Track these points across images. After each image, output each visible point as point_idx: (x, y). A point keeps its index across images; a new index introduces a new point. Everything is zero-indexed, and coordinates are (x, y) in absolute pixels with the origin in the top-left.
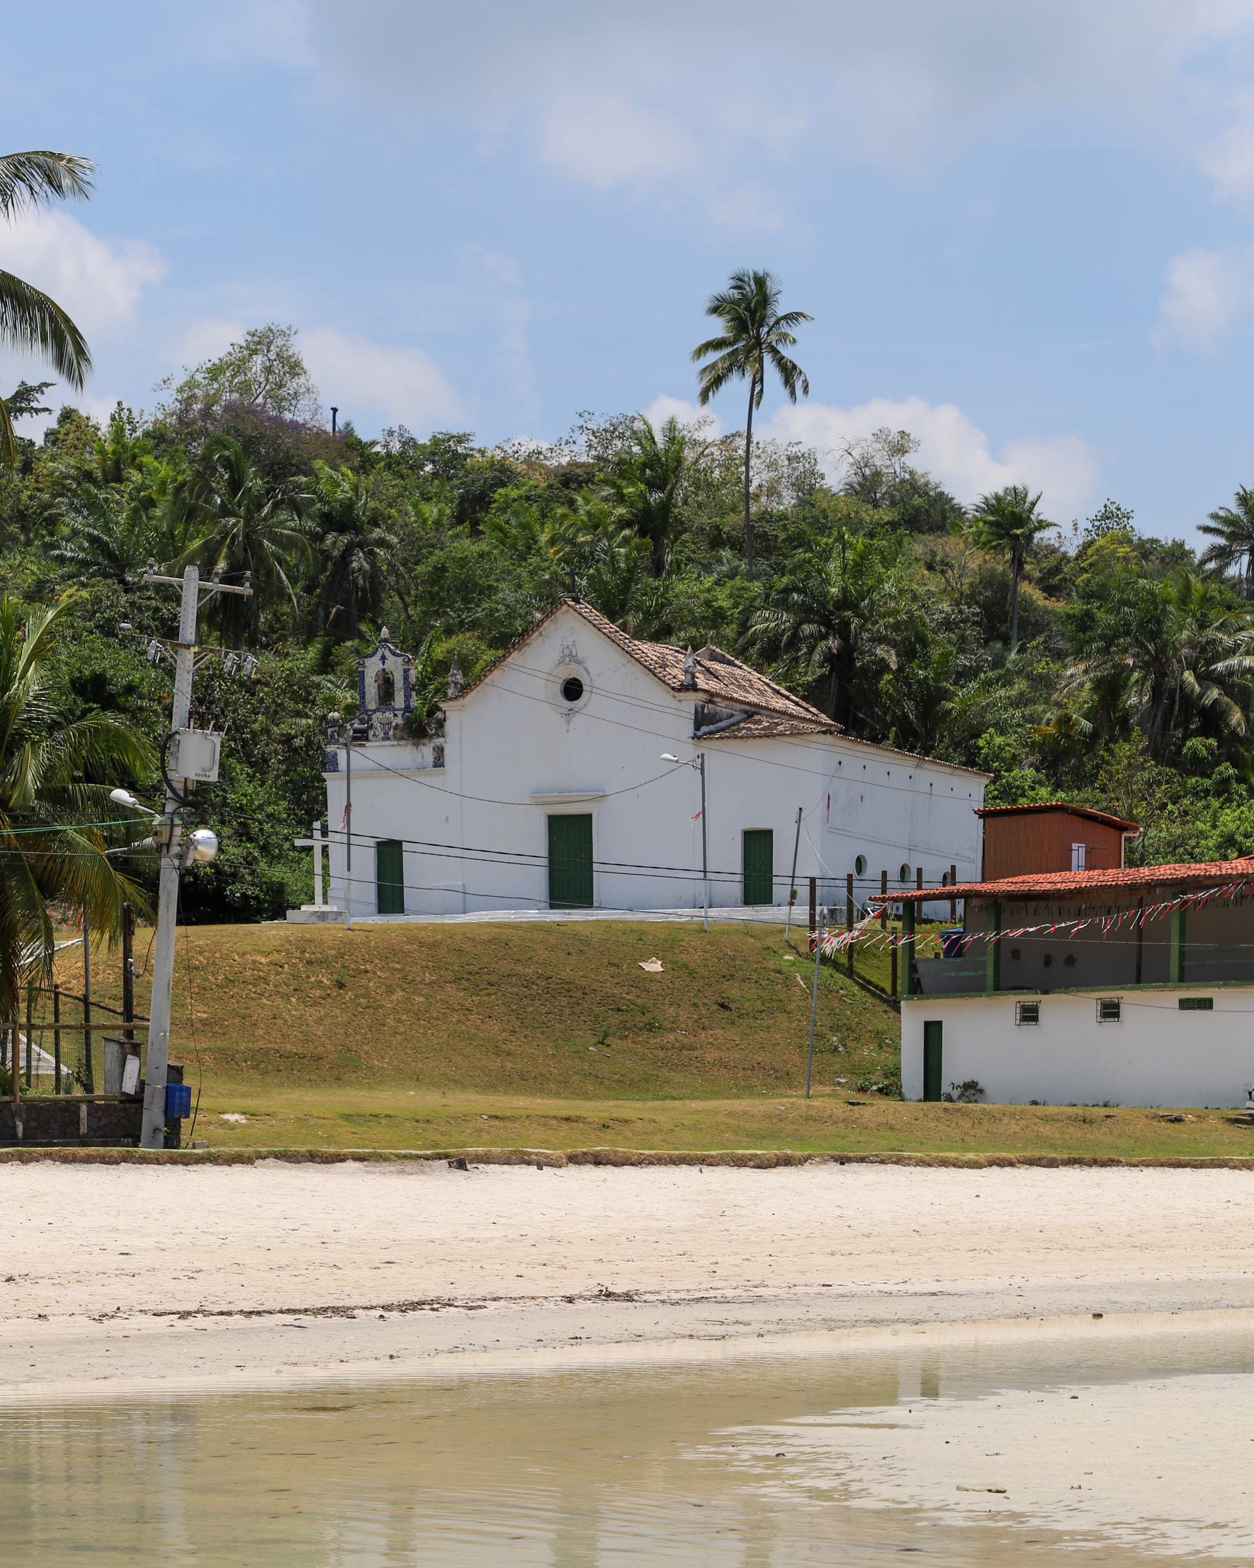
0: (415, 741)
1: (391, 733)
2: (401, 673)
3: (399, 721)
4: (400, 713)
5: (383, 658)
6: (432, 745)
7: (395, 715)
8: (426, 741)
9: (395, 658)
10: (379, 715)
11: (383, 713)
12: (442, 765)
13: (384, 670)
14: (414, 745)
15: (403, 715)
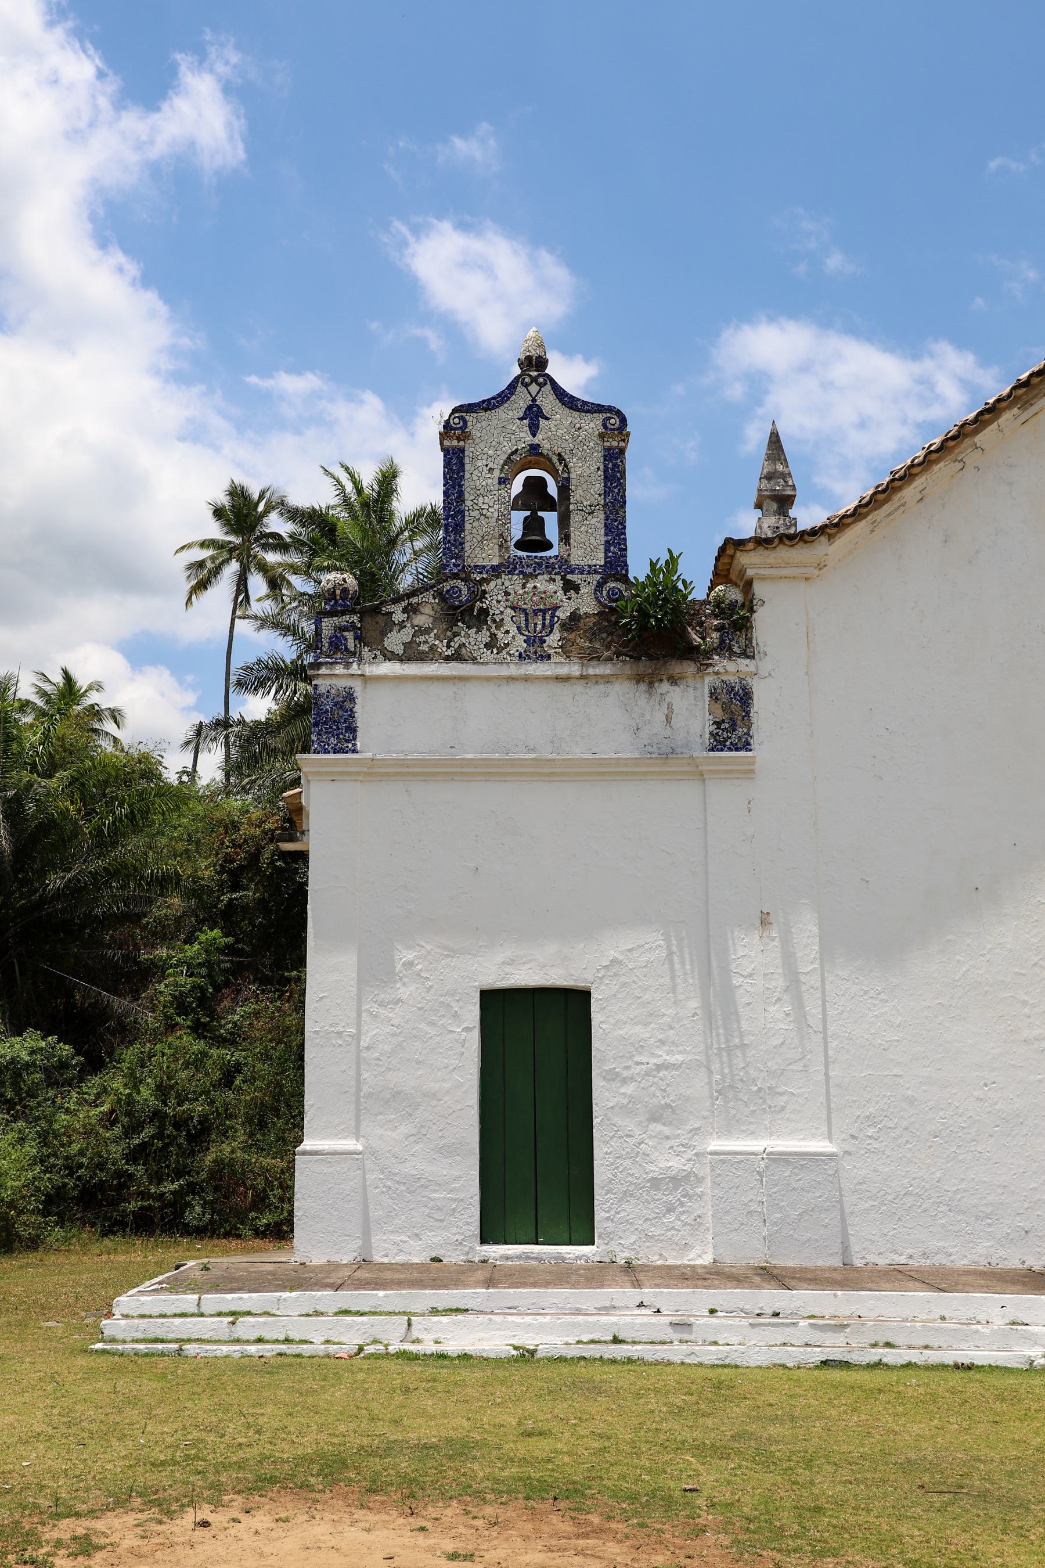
0: (645, 666)
1: (553, 639)
2: (596, 460)
3: (586, 603)
5: (534, 415)
7: (570, 587)
8: (689, 668)
10: (513, 583)
11: (528, 577)
12: (747, 746)
13: (534, 448)
14: (639, 679)
15: (600, 586)
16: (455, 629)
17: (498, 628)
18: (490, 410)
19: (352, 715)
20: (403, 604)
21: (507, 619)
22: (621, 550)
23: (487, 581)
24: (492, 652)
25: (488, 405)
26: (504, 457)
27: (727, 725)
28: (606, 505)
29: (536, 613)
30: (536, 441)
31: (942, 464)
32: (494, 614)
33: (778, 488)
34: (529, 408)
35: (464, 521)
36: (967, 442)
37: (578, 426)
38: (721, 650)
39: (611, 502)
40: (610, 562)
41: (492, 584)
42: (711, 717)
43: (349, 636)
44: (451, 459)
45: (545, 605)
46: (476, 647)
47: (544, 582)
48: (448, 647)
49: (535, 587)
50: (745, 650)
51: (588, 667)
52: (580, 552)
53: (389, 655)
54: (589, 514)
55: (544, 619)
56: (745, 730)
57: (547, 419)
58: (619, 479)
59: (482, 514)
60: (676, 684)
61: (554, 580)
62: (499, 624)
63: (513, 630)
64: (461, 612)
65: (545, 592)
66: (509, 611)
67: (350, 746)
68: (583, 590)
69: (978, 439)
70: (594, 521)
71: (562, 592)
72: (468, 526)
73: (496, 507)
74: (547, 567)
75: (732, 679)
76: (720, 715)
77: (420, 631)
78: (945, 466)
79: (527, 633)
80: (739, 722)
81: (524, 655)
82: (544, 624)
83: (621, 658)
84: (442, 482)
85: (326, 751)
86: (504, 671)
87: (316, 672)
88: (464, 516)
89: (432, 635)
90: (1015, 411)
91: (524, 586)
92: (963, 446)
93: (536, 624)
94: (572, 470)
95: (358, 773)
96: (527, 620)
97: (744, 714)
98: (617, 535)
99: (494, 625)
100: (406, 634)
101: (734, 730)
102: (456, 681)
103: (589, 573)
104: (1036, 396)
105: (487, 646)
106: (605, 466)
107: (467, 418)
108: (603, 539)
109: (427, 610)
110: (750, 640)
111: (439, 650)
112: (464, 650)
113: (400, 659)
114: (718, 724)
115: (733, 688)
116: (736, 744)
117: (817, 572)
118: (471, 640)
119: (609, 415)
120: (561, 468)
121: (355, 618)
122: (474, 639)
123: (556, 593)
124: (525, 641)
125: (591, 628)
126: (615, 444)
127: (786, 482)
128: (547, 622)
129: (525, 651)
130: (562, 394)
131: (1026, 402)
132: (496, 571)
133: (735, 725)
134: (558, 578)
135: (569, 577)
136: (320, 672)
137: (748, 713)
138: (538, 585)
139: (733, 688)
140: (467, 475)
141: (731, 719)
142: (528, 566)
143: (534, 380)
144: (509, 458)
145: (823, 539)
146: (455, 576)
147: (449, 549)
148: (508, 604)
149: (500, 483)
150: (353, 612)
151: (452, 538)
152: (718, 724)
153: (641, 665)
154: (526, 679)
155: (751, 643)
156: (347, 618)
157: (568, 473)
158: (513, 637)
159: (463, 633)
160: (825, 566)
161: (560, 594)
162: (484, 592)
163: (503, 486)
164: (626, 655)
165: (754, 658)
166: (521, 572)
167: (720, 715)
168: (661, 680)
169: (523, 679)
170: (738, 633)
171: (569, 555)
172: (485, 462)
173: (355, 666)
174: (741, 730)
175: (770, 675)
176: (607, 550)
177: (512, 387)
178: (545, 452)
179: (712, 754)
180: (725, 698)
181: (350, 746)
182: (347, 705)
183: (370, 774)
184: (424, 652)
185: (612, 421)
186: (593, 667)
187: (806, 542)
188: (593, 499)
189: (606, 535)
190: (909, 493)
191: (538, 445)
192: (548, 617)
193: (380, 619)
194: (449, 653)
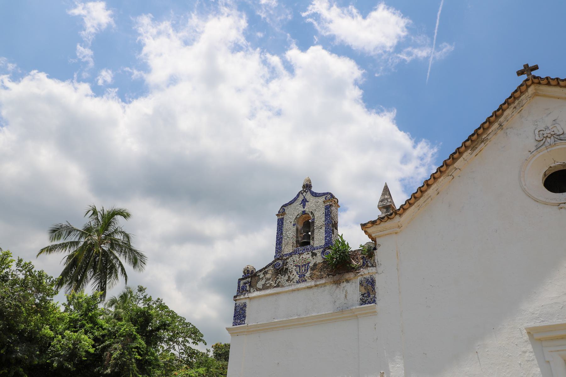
0: (336, 277)
1: (308, 274)
2: (323, 210)
3: (319, 259)
4: (318, 252)
6: (359, 278)
7: (314, 254)
8: (351, 275)
9: (317, 199)
10: (296, 257)
11: (300, 254)
13: (304, 212)
15: (323, 252)
16: (277, 277)
17: (290, 274)
18: (291, 204)
20: (263, 271)
21: (294, 270)
22: (330, 238)
23: (288, 258)
25: (291, 203)
26: (295, 217)
27: (366, 295)
28: (325, 224)
30: (305, 209)
31: (442, 178)
32: (290, 269)
33: (385, 204)
34: (303, 200)
35: (282, 241)
36: (451, 167)
37: (317, 201)
38: (364, 266)
39: (327, 223)
40: (326, 243)
41: (290, 259)
42: (360, 293)
43: (247, 285)
44: (279, 222)
45: (306, 263)
46: (283, 282)
47: (306, 255)
49: (303, 257)
50: (373, 265)
51: (317, 281)
52: (317, 242)
53: (258, 289)
54: (320, 228)
55: (305, 268)
56: (373, 296)
57: (308, 202)
58: (330, 215)
59: (288, 237)
60: (349, 282)
61: (309, 254)
62: (291, 272)
63: (295, 273)
64: (280, 270)
65: (306, 258)
66: (295, 267)
67: (243, 322)
69: (456, 165)
71: (311, 257)
72: (283, 242)
73: (292, 233)
74: (307, 250)
75: (367, 276)
76: (364, 291)
78: (444, 178)
80: (371, 293)
81: (298, 282)
82: (305, 269)
83: (329, 276)
84: (276, 229)
85: (236, 325)
86: (293, 287)
88: (282, 239)
89: (271, 280)
90: (469, 151)
91: (299, 258)
92: (449, 169)
94: (315, 216)
95: (244, 332)
96: (300, 269)
97: (372, 289)
98: (329, 234)
100: (263, 282)
101: (369, 297)
102: (277, 295)
103: (320, 248)
104: (477, 144)
105: (287, 281)
106: (325, 211)
107: (285, 208)
108: (325, 236)
109: (270, 272)
110: (374, 260)
111: (272, 285)
113: (260, 290)
114: (363, 295)
115: (368, 280)
116: (370, 302)
117: (398, 230)
118: (282, 279)
119: (327, 195)
120: (312, 216)
121: (249, 279)
122: (283, 279)
123: (309, 258)
124: (299, 277)
125: (320, 268)
126: (328, 204)
127: (388, 201)
129: (299, 280)
130: (312, 193)
131: (474, 147)
132: (291, 255)
133: (369, 294)
135: (313, 251)
136: (237, 299)
137: (374, 289)
138: (304, 256)
139: (368, 280)
140: (284, 226)
141: (368, 292)
142: (300, 251)
143: (305, 191)
144: (296, 217)
145: (397, 216)
146: (278, 259)
147: (277, 250)
148: (294, 265)
149: (293, 226)
150: (249, 277)
151: (278, 247)
152: (363, 295)
153: (335, 277)
154: (298, 290)
155: (375, 261)
156: (247, 280)
157: (314, 217)
158: (295, 276)
159: (280, 278)
160: (402, 226)
161: (311, 258)
162: (287, 262)
163: (294, 226)
164: (332, 275)
165: (376, 267)
166: (298, 253)
167: (364, 291)
168: (343, 282)
170: (371, 259)
171: (314, 244)
172: (289, 220)
173: (246, 295)
174: (372, 296)
175: (383, 272)
176: (326, 239)
177: (298, 195)
178: (307, 212)
180: (365, 284)
181: (243, 322)
184: (268, 287)
185: (328, 197)
186: (319, 281)
187: (391, 219)
188: (321, 223)
189: (325, 234)
190: (431, 191)
191: (305, 211)
192: (306, 267)
193: (257, 278)
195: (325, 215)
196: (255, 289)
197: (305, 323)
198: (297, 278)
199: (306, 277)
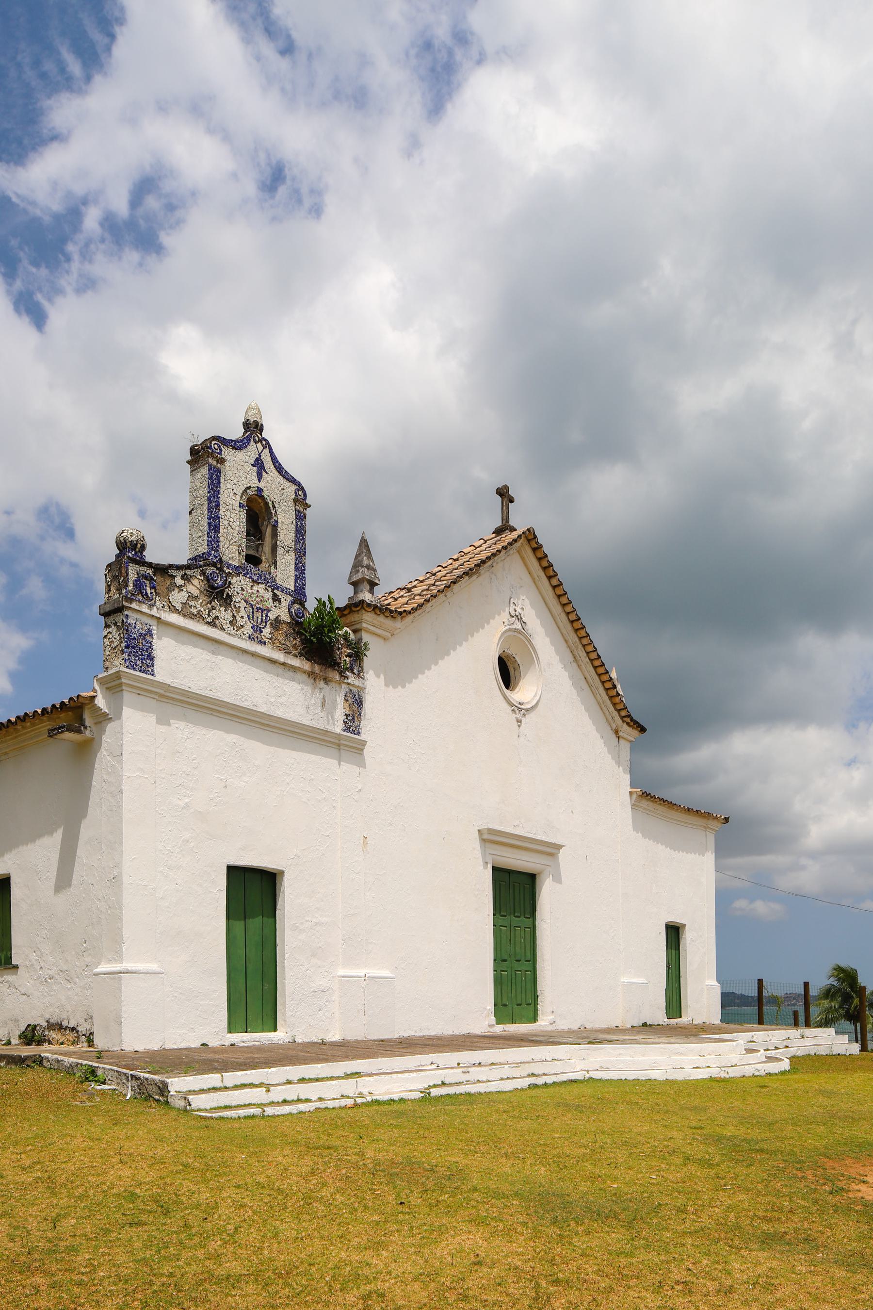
1: (267, 631)
3: (282, 612)
4: (286, 600)
7: (276, 598)
11: (255, 582)
14: (311, 674)
19: (151, 647)
21: (242, 608)
24: (234, 629)
29: (258, 609)
32: (235, 602)
48: (209, 615)
51: (288, 658)
60: (327, 684)
62: (238, 609)
64: (216, 593)
67: (150, 670)
68: (283, 604)
70: (289, 558)
77: (192, 597)
79: (252, 622)
80: (356, 718)
82: (262, 619)
87: (129, 605)
93: (258, 618)
95: (156, 693)
96: (253, 613)
99: (235, 610)
102: (214, 643)
112: (217, 622)
122: (225, 615)
123: (268, 599)
128: (264, 618)
134: (270, 590)
135: (275, 591)
141: (353, 715)
148: (243, 597)
154: (254, 655)
161: (271, 600)
166: (251, 577)
169: (251, 654)
176: (296, 582)
179: (345, 733)
182: (148, 638)
183: (162, 696)
186: (291, 659)
189: (296, 570)
194: (209, 620)
195: (296, 530)
196: (166, 604)
197: (268, 725)
198: (248, 629)
199: (264, 636)
